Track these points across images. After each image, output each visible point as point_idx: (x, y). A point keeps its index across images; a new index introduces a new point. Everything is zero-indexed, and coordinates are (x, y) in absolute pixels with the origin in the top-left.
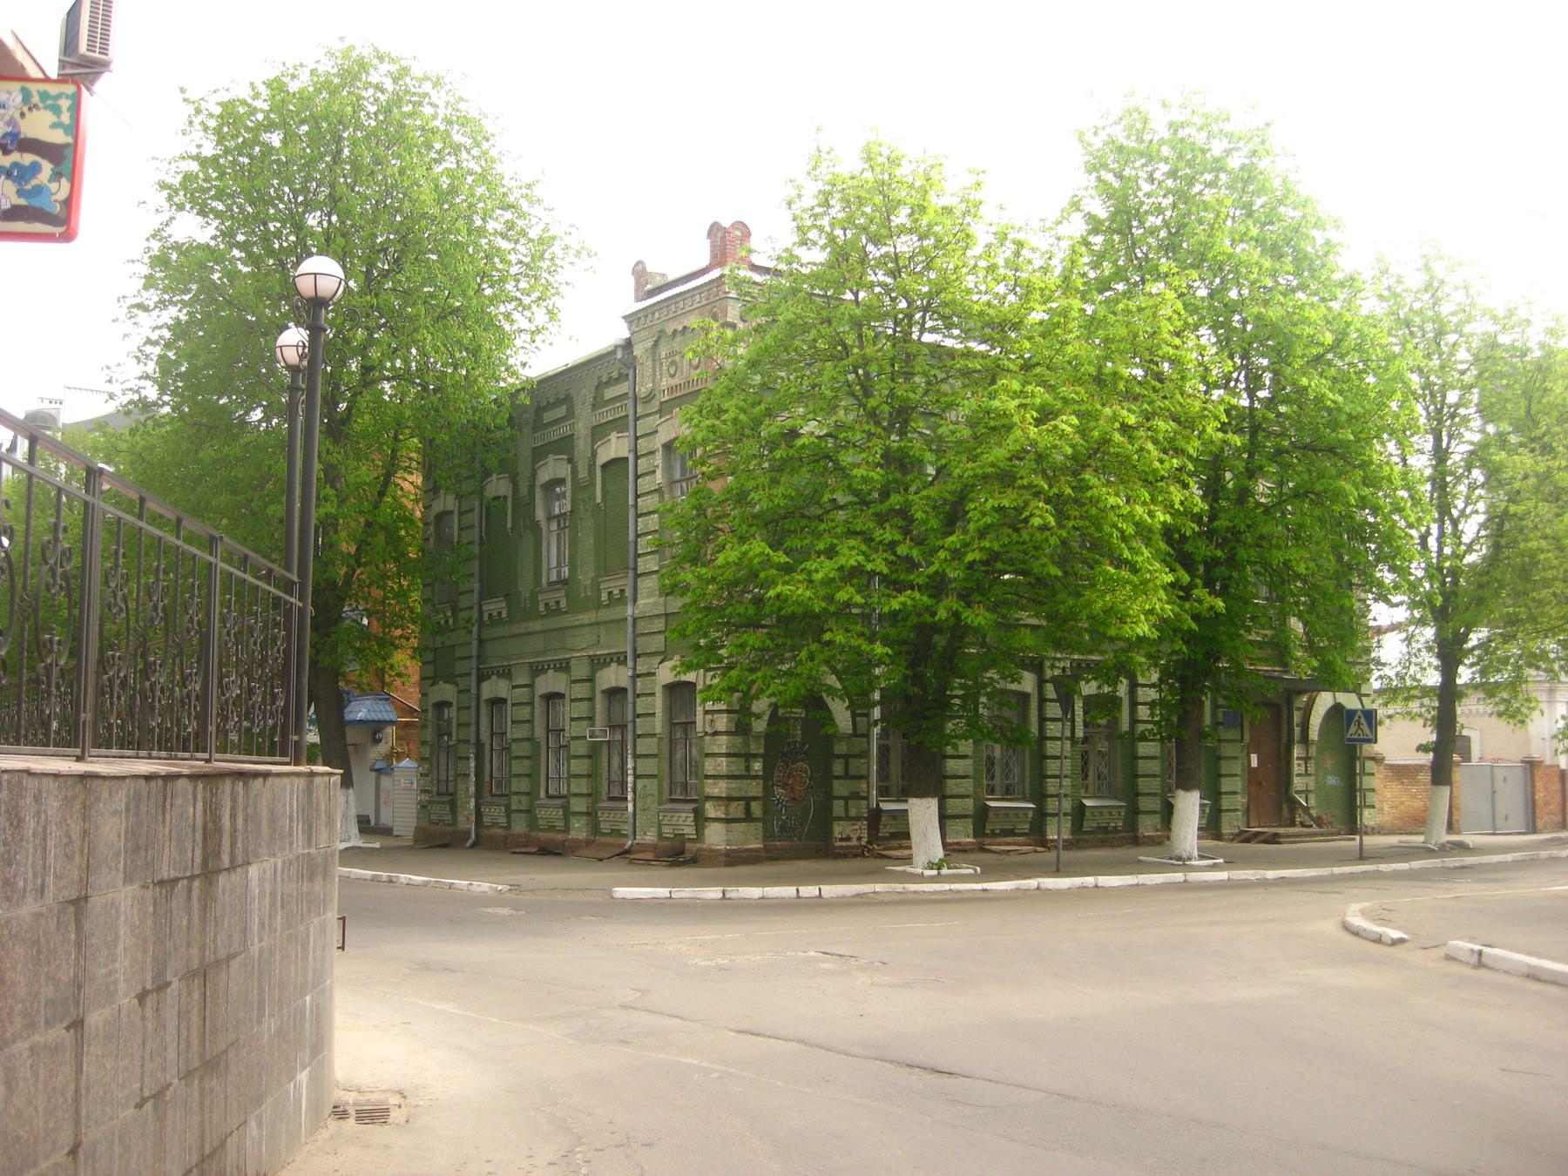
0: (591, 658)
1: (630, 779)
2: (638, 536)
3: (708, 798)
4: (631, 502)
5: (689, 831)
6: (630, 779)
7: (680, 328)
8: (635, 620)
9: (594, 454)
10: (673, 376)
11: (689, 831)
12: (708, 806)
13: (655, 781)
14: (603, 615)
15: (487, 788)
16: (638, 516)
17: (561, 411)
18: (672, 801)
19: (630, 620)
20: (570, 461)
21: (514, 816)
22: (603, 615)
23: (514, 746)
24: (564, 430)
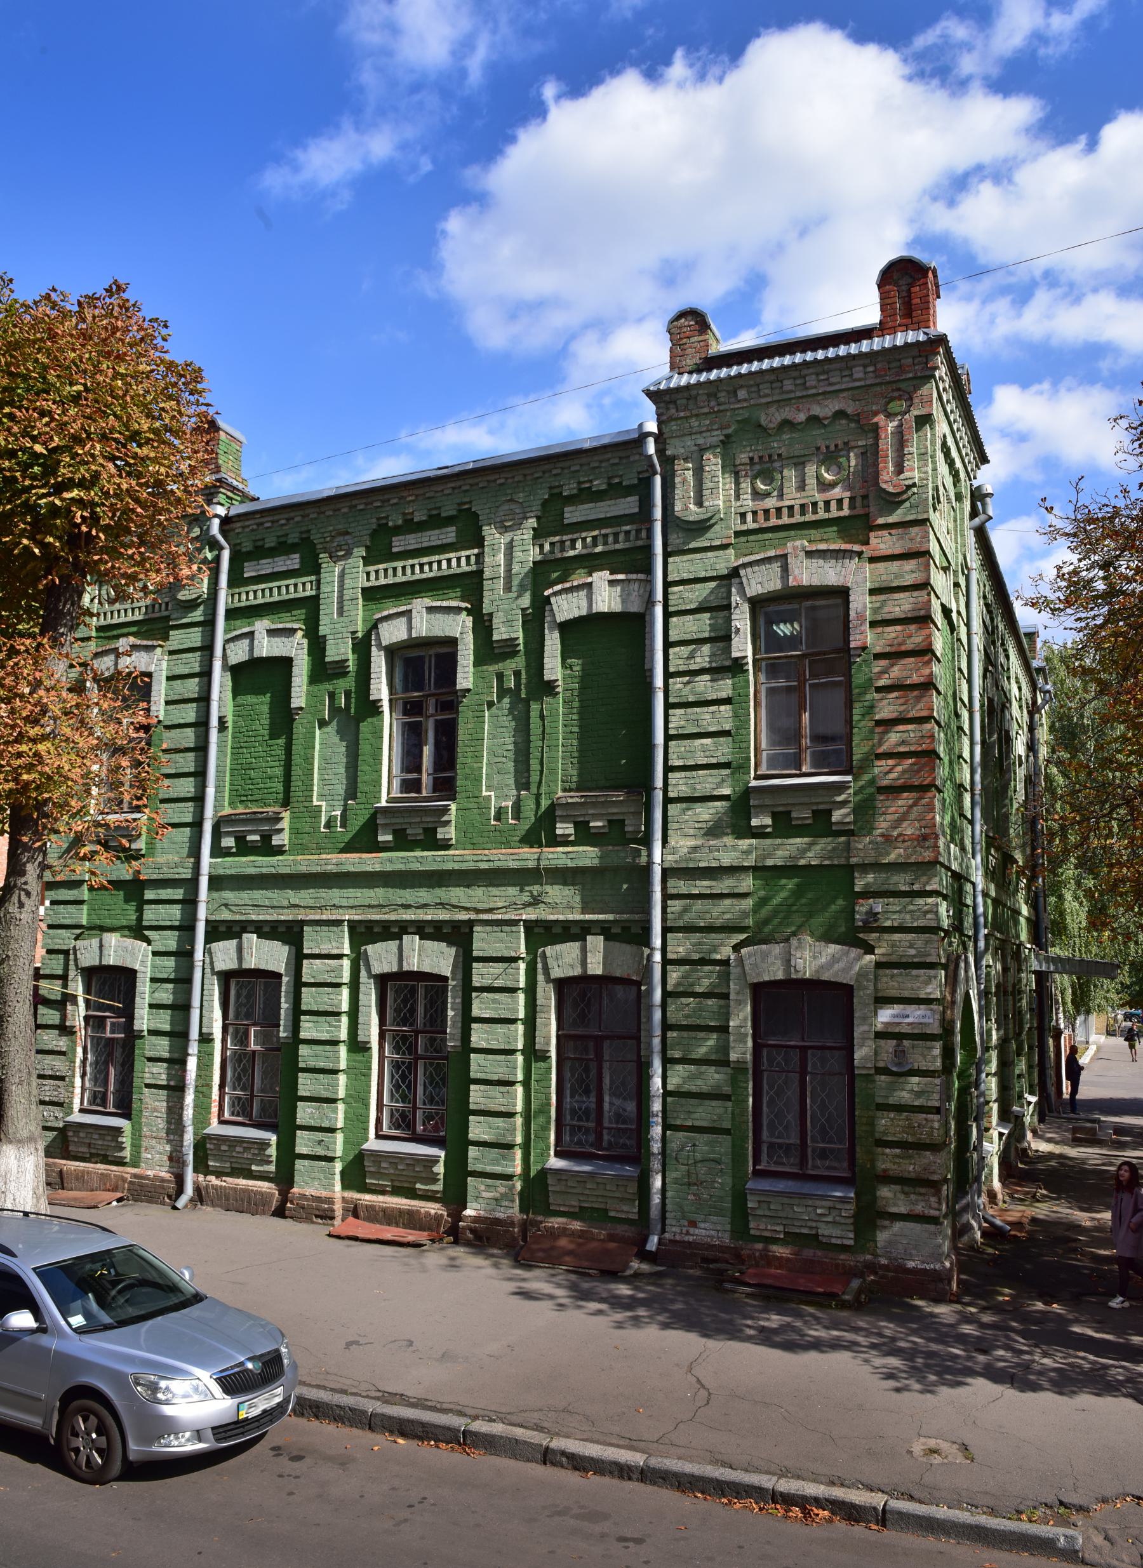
0: (530, 926)
1: (657, 1131)
2: (668, 738)
3: (887, 1179)
4: (659, 682)
5: (838, 1233)
6: (657, 1131)
7: (801, 417)
8: (664, 871)
9: (541, 605)
10: (767, 495)
11: (838, 1233)
12: (885, 1192)
13: (726, 1140)
14: (556, 856)
15: (215, 1110)
16: (668, 706)
17: (449, 534)
18: (757, 1174)
19: (657, 871)
20: (469, 612)
21: (299, 1164)
22: (556, 856)
23: (303, 1050)
24: (459, 562)
